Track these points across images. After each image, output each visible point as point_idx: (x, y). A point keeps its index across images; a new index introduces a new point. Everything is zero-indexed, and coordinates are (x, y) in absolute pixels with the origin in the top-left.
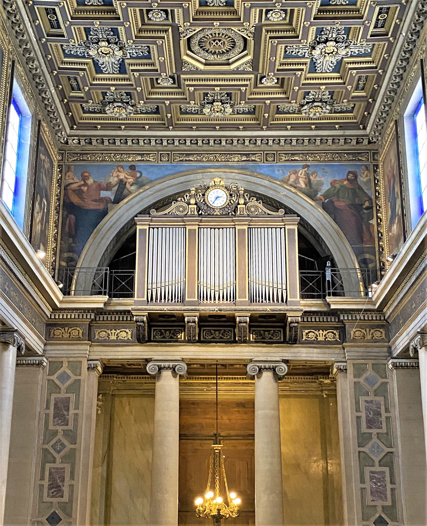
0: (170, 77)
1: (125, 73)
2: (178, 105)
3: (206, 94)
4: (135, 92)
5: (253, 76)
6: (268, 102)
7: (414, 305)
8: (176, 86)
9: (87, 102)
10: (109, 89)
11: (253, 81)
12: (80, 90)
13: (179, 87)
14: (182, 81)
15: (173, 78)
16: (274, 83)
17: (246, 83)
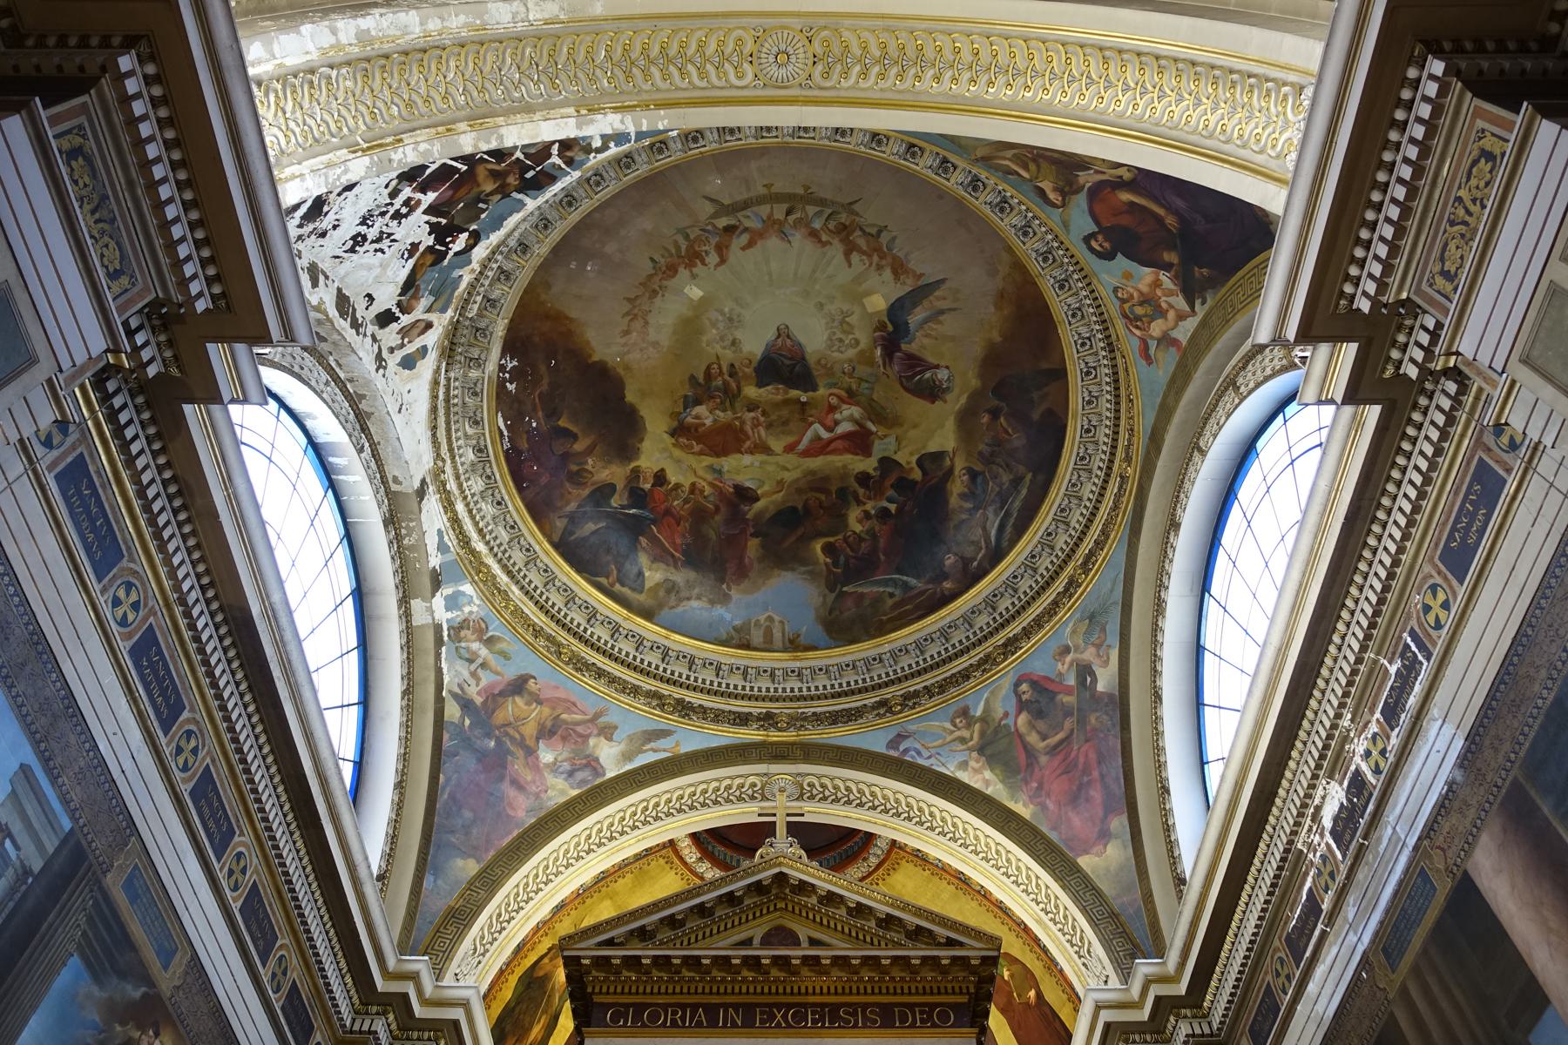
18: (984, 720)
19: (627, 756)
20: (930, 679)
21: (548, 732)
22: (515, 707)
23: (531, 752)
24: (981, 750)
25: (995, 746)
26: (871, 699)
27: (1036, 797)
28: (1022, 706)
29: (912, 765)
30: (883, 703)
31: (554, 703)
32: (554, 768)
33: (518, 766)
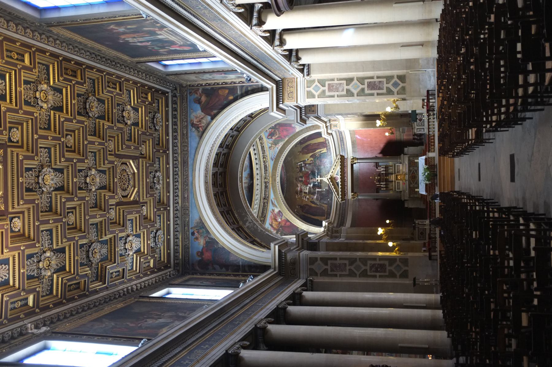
0: (11, 221)
1: (9, 259)
2: (40, 214)
3: (28, 190)
4: (26, 250)
5: (9, 150)
6: (36, 137)
7: (200, 7)
8: (21, 215)
9: (38, 292)
10: (23, 273)
11: (13, 149)
12: (27, 299)
13: (23, 213)
14: (14, 210)
15: (12, 219)
16: (17, 132)
17: (15, 155)
18: (272, 144)
19: (276, 207)
20: (261, 152)
21: (276, 220)
22: (275, 226)
23: (280, 223)
24: (276, 145)
25: (275, 143)
26: (262, 163)
27: (285, 137)
28: (271, 138)
29: (277, 157)
30: (264, 162)
31: (272, 219)
32: (281, 219)
33: (283, 224)
